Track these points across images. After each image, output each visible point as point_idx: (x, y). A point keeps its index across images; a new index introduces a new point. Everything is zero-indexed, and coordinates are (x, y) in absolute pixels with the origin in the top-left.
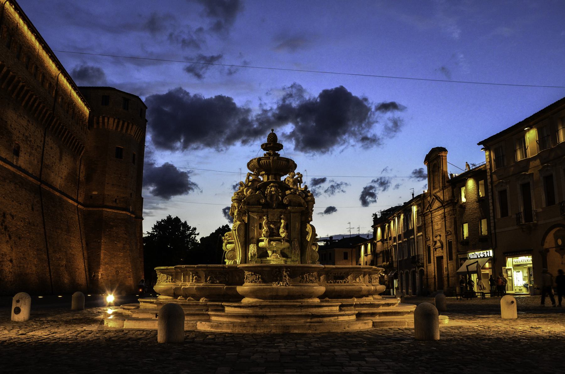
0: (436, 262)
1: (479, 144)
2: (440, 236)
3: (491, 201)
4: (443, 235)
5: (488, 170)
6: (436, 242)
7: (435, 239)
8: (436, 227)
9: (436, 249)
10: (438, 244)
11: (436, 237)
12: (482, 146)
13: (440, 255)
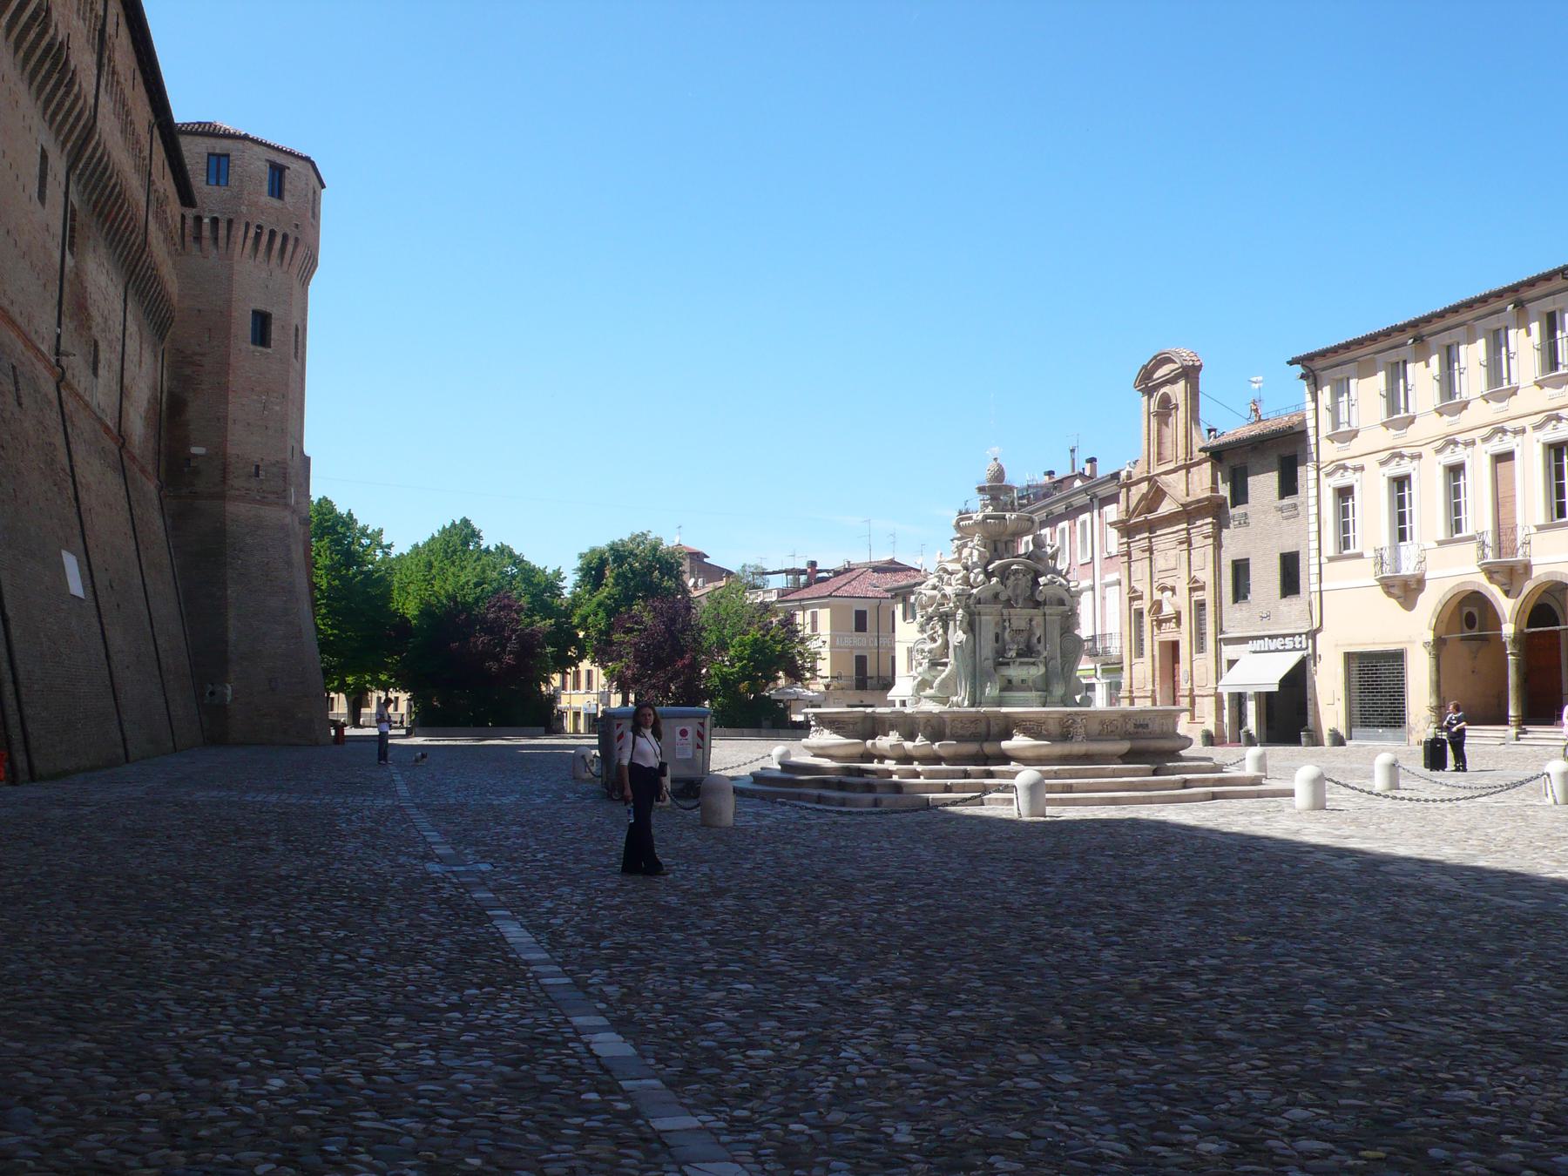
0: (1157, 653)
1: (1291, 363)
2: (1173, 590)
3: (1313, 510)
4: (1183, 587)
5: (1311, 432)
6: (1157, 606)
7: (1157, 595)
8: (1160, 562)
9: (1160, 623)
10: (1168, 610)
11: (1163, 589)
12: (1298, 370)
13: (1170, 637)
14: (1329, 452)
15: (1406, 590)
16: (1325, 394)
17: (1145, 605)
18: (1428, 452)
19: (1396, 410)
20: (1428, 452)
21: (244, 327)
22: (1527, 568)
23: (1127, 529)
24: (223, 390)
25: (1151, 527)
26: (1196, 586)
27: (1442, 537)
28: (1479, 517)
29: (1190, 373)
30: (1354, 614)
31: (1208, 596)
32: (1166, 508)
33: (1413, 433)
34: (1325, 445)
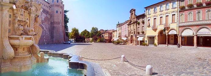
10: (132, 32)
14: (148, 16)
15: (155, 30)
16: (148, 10)
17: (130, 32)
18: (158, 16)
19: (155, 12)
20: (158, 16)
21: (55, 12)
22: (170, 27)
23: (128, 25)
24: (54, 17)
25: (131, 24)
26: (134, 30)
27: (159, 24)
28: (164, 22)
29: (135, 10)
30: (150, 32)
31: (135, 31)
32: (132, 22)
33: (157, 14)
34: (147, 16)
